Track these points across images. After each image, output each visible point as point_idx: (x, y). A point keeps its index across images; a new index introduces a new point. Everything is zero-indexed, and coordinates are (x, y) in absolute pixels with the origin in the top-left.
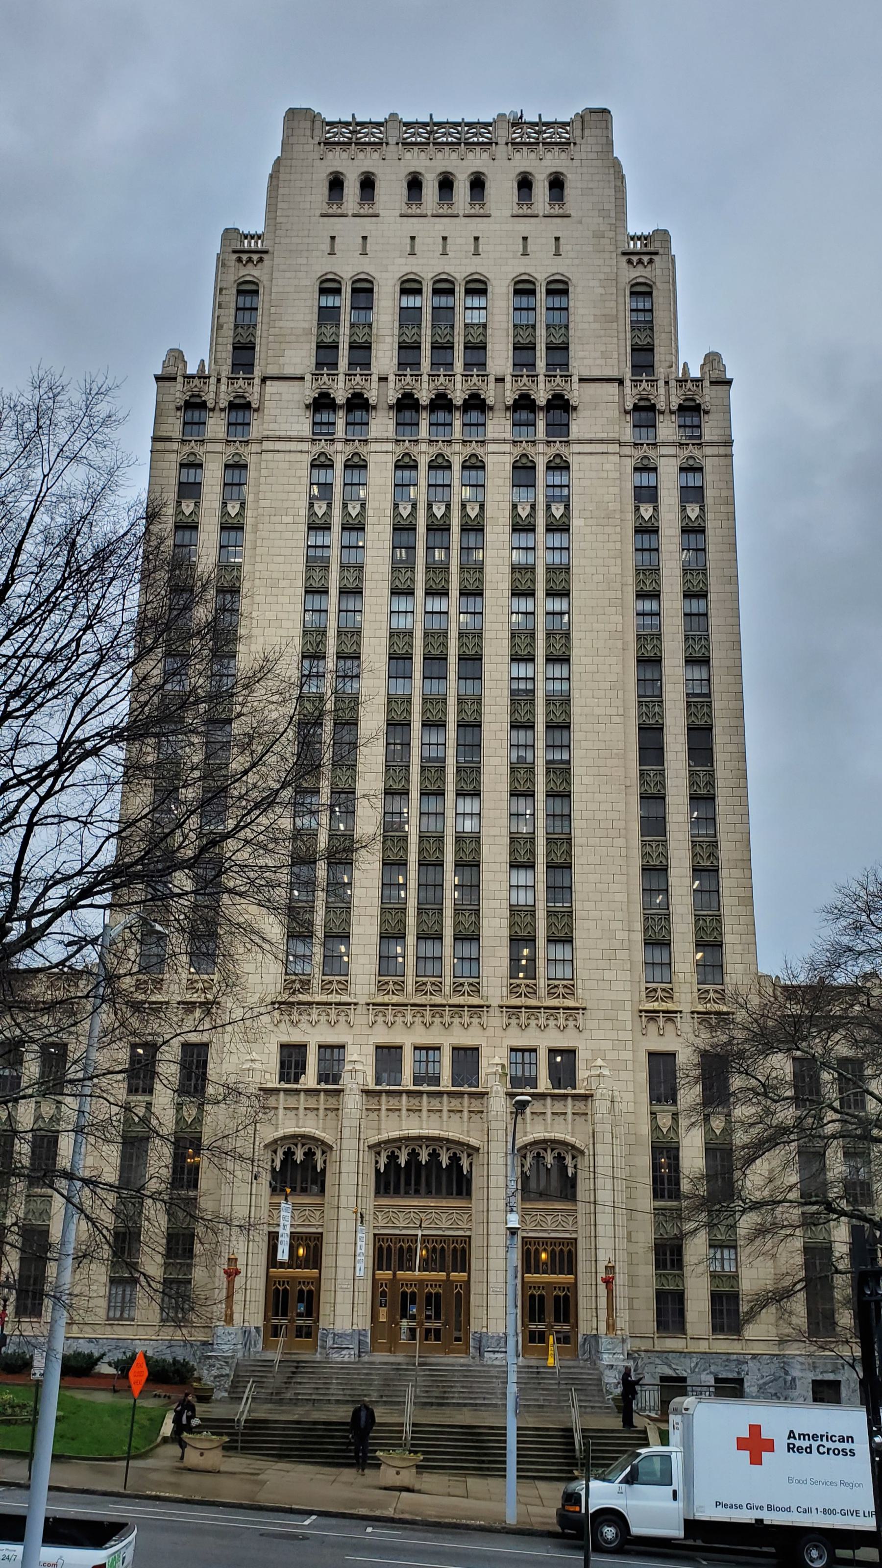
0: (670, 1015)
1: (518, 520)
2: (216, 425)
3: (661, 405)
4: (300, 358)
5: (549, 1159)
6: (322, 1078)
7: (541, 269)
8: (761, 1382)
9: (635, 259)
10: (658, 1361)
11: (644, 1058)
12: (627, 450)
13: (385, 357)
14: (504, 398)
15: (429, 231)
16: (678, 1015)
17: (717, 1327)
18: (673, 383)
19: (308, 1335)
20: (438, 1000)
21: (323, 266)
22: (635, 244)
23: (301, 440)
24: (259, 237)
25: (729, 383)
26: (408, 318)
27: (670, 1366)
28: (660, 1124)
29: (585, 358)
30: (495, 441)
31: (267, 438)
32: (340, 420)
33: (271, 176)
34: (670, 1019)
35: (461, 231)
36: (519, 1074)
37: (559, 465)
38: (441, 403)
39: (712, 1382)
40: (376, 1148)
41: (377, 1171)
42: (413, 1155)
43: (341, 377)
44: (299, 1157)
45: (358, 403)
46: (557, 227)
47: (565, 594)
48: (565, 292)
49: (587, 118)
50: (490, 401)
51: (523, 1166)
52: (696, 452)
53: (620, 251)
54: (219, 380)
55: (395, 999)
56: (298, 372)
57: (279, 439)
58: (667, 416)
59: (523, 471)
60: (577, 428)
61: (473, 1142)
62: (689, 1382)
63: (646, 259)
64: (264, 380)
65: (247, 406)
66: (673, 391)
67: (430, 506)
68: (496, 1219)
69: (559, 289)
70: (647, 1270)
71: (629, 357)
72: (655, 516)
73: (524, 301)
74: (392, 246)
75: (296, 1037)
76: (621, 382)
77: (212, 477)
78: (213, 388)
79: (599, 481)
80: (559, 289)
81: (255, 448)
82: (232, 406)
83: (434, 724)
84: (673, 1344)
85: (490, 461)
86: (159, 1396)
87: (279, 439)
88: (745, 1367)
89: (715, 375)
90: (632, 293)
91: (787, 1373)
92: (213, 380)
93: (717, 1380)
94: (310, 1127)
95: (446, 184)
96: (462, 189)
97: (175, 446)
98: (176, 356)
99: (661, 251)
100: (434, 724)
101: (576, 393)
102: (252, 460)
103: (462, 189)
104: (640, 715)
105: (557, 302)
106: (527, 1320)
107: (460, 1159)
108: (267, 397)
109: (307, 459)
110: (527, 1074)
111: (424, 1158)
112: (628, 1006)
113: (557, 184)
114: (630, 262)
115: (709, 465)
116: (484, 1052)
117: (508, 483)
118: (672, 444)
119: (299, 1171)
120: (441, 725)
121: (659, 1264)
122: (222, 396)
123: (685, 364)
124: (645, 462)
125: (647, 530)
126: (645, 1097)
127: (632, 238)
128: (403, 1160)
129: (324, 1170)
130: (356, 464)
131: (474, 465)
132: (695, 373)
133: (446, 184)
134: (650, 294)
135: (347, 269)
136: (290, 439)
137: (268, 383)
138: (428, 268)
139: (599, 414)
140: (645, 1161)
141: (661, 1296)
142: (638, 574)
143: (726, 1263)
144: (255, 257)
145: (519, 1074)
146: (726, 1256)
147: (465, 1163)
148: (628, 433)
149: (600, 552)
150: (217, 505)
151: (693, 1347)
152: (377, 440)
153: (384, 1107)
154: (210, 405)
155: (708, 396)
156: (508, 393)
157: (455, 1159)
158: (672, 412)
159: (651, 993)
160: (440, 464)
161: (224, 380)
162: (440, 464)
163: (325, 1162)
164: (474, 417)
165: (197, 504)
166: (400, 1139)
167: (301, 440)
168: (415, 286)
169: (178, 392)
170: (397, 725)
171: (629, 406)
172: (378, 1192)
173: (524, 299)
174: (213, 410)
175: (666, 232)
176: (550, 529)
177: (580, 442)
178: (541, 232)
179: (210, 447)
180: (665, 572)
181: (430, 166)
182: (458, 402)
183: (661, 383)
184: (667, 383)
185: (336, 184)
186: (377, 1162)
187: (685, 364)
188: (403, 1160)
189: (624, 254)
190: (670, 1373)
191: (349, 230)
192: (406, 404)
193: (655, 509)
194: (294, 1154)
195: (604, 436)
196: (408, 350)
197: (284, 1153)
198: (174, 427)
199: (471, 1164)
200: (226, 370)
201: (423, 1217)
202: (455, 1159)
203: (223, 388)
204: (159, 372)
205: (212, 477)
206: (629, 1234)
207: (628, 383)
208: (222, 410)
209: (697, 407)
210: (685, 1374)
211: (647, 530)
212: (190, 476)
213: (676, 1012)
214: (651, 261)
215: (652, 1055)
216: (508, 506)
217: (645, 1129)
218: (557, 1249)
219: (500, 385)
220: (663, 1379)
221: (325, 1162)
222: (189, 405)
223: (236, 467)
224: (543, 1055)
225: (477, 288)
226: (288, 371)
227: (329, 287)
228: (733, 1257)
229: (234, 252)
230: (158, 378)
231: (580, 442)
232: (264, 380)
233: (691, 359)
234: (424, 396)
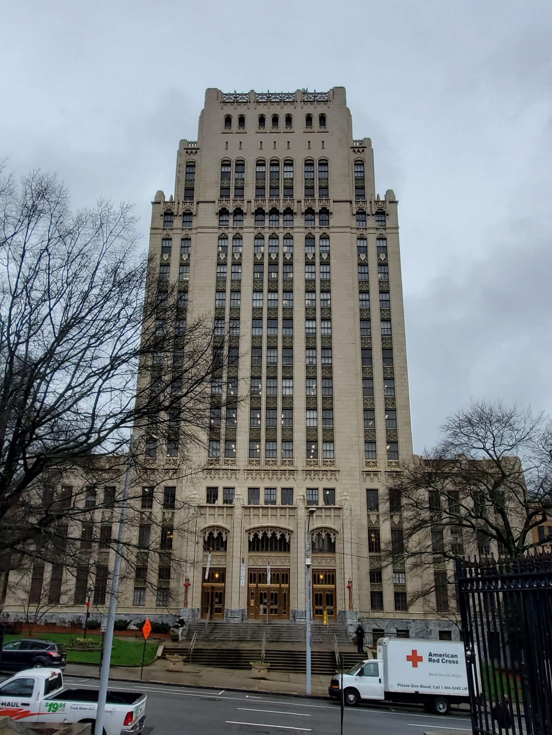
0: (376, 473)
1: (308, 260)
2: (178, 222)
3: (368, 212)
4: (214, 193)
5: (324, 535)
6: (225, 501)
7: (316, 155)
8: (417, 631)
9: (356, 150)
10: (372, 622)
11: (365, 492)
12: (354, 231)
13: (250, 193)
14: (301, 209)
15: (268, 139)
16: (379, 473)
17: (397, 608)
18: (373, 203)
19: (220, 612)
20: (275, 468)
21: (223, 154)
22: (356, 144)
23: (214, 228)
24: (195, 143)
25: (396, 202)
26: (260, 176)
28: (372, 519)
29: (334, 193)
30: (297, 227)
31: (200, 227)
32: (231, 219)
33: (200, 117)
34: (376, 475)
35: (282, 139)
36: (311, 499)
37: (325, 237)
38: (274, 211)
39: (395, 632)
40: (249, 531)
41: (249, 541)
42: (265, 534)
43: (231, 201)
44: (215, 535)
45: (239, 212)
46: (323, 136)
47: (329, 291)
48: (326, 164)
49: (335, 90)
50: (295, 211)
51: (312, 538)
52: (383, 232)
53: (350, 146)
54: (179, 203)
55: (256, 468)
56: (212, 200)
57: (205, 227)
58: (371, 217)
59: (310, 239)
60: (333, 221)
61: (291, 528)
62: (385, 632)
63: (361, 150)
64: (198, 203)
65: (191, 214)
66: (373, 206)
67: (270, 255)
68: (301, 561)
69: (324, 163)
70: (367, 582)
71: (354, 192)
72: (366, 259)
73: (309, 168)
74: (252, 145)
75: (213, 484)
76: (351, 202)
77: (176, 244)
78: (176, 207)
79: (342, 245)
80: (324, 163)
81: (194, 231)
82: (185, 214)
83: (272, 348)
85: (295, 236)
86: (156, 639)
87: (205, 227)
88: (409, 625)
89: (391, 200)
90: (355, 164)
91: (428, 628)
92: (176, 203)
93: (398, 631)
94: (220, 522)
95: (275, 119)
96: (282, 121)
97: (160, 231)
98: (160, 194)
99: (367, 146)
100: (272, 348)
101: (332, 207)
102: (193, 237)
103: (282, 121)
105: (323, 168)
106: (314, 604)
107: (285, 536)
108: (199, 210)
109: (217, 236)
110: (314, 499)
111: (269, 535)
112: (358, 469)
113: (323, 119)
114: (354, 151)
115: (389, 237)
116: (295, 490)
117: (304, 245)
118: (374, 228)
119: (216, 541)
120: (276, 348)
121: (372, 580)
122: (180, 210)
123: (378, 195)
124: (362, 236)
125: (363, 264)
126: (365, 508)
127: (355, 141)
129: (226, 541)
130: (238, 237)
131: (288, 237)
132: (382, 198)
133: (275, 119)
134: (363, 165)
135: (233, 155)
136: (209, 228)
137: (200, 204)
138: (268, 156)
139: (342, 216)
140: (365, 535)
141: (373, 594)
142: (359, 283)
144: (194, 151)
145: (311, 499)
146: (400, 577)
147: (287, 537)
148: (354, 224)
149: (343, 275)
150: (179, 256)
152: (246, 227)
153: (252, 514)
154: (175, 213)
155: (388, 208)
156: (303, 207)
157: (283, 536)
158: (373, 215)
159: (367, 464)
160: (274, 237)
161: (181, 203)
162: (274, 237)
163: (227, 538)
164: (288, 217)
165: (170, 255)
166: (259, 528)
167: (214, 228)
168: (263, 162)
169: (161, 209)
170: (256, 349)
171: (355, 213)
172: (249, 550)
173: (309, 167)
174: (176, 216)
175: (369, 139)
176: (322, 264)
177: (333, 227)
178: (316, 138)
179: (175, 231)
180: (371, 282)
181: (268, 112)
182: (281, 211)
183: (368, 202)
184: (371, 202)
185: (228, 120)
186: (249, 537)
187: (378, 195)
188: (260, 536)
189: (352, 148)
190: (376, 627)
191: (234, 139)
192: (259, 212)
193: (367, 255)
194: (213, 534)
195: (344, 225)
196: (260, 188)
197: (209, 534)
198: (160, 223)
199: (290, 538)
200: (182, 199)
201: (269, 561)
202: (283, 536)
203: (181, 206)
204: (153, 200)
205: (176, 244)
206: (358, 567)
207: (354, 203)
208: (180, 216)
209: (385, 211)
210: (383, 628)
211: (363, 264)
212: (167, 244)
213: (378, 472)
214: (363, 151)
215: (368, 490)
216: (304, 255)
217: (365, 522)
218: (327, 574)
219: (299, 204)
220: (374, 630)
221: (227, 538)
222: (166, 214)
224: (321, 492)
225: (289, 163)
226: (208, 199)
227: (225, 163)
228: (403, 577)
229: (185, 149)
230: (153, 203)
231: (333, 227)
233: (380, 192)
234: (267, 209)
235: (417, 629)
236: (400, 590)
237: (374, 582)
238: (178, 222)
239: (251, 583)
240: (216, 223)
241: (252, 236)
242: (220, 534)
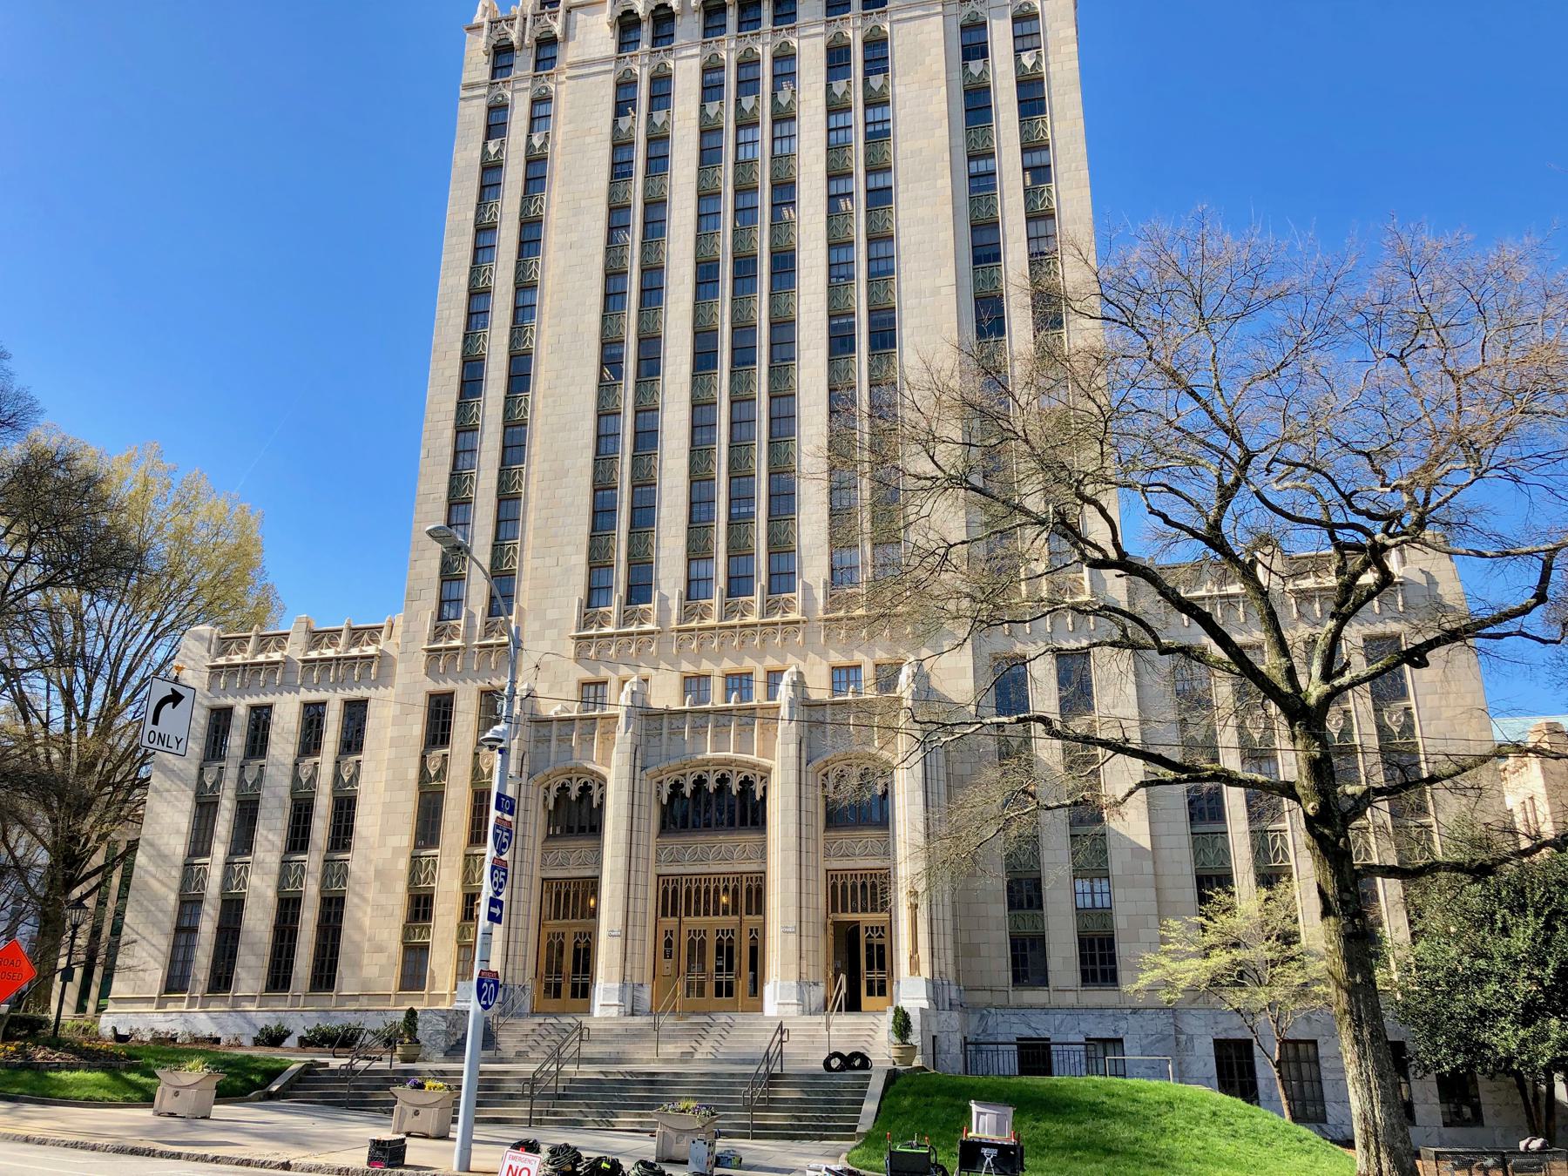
2: (523, 64)
8: (1145, 1042)
10: (1013, 1019)
27: (1029, 1026)
51: (824, 786)
70: (1000, 909)
84: (1031, 996)
88: (1123, 1024)
91: (1178, 1031)
92: (517, 24)
97: (484, 91)
104: (976, 282)
109: (610, 80)
121: (1013, 905)
128: (688, 790)
143: (1097, 897)
146: (1097, 889)
151: (1058, 999)
167: (605, 60)
223: (541, 101)
228: (1105, 889)
232: (568, 12)
235: (1147, 1036)
236: (1095, 928)
237: (1021, 907)
238: (523, 64)
239: (664, 914)
240: (610, 47)
241: (695, 65)
242: (585, 789)
